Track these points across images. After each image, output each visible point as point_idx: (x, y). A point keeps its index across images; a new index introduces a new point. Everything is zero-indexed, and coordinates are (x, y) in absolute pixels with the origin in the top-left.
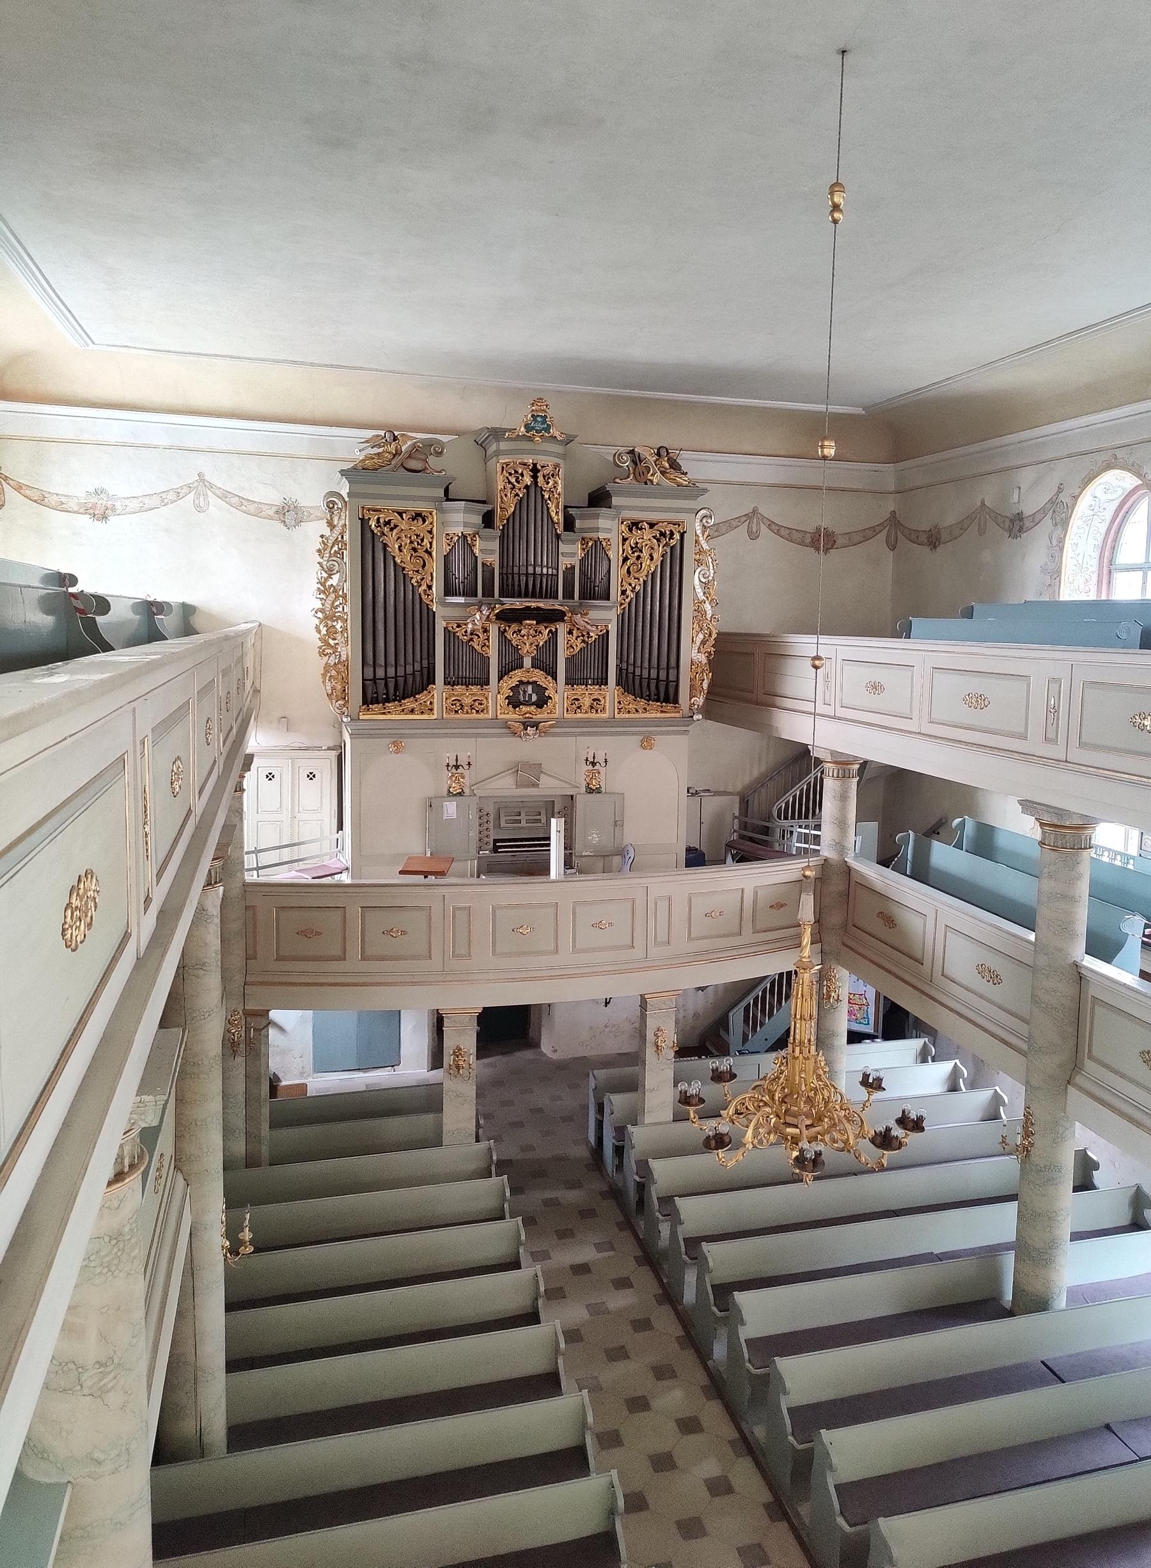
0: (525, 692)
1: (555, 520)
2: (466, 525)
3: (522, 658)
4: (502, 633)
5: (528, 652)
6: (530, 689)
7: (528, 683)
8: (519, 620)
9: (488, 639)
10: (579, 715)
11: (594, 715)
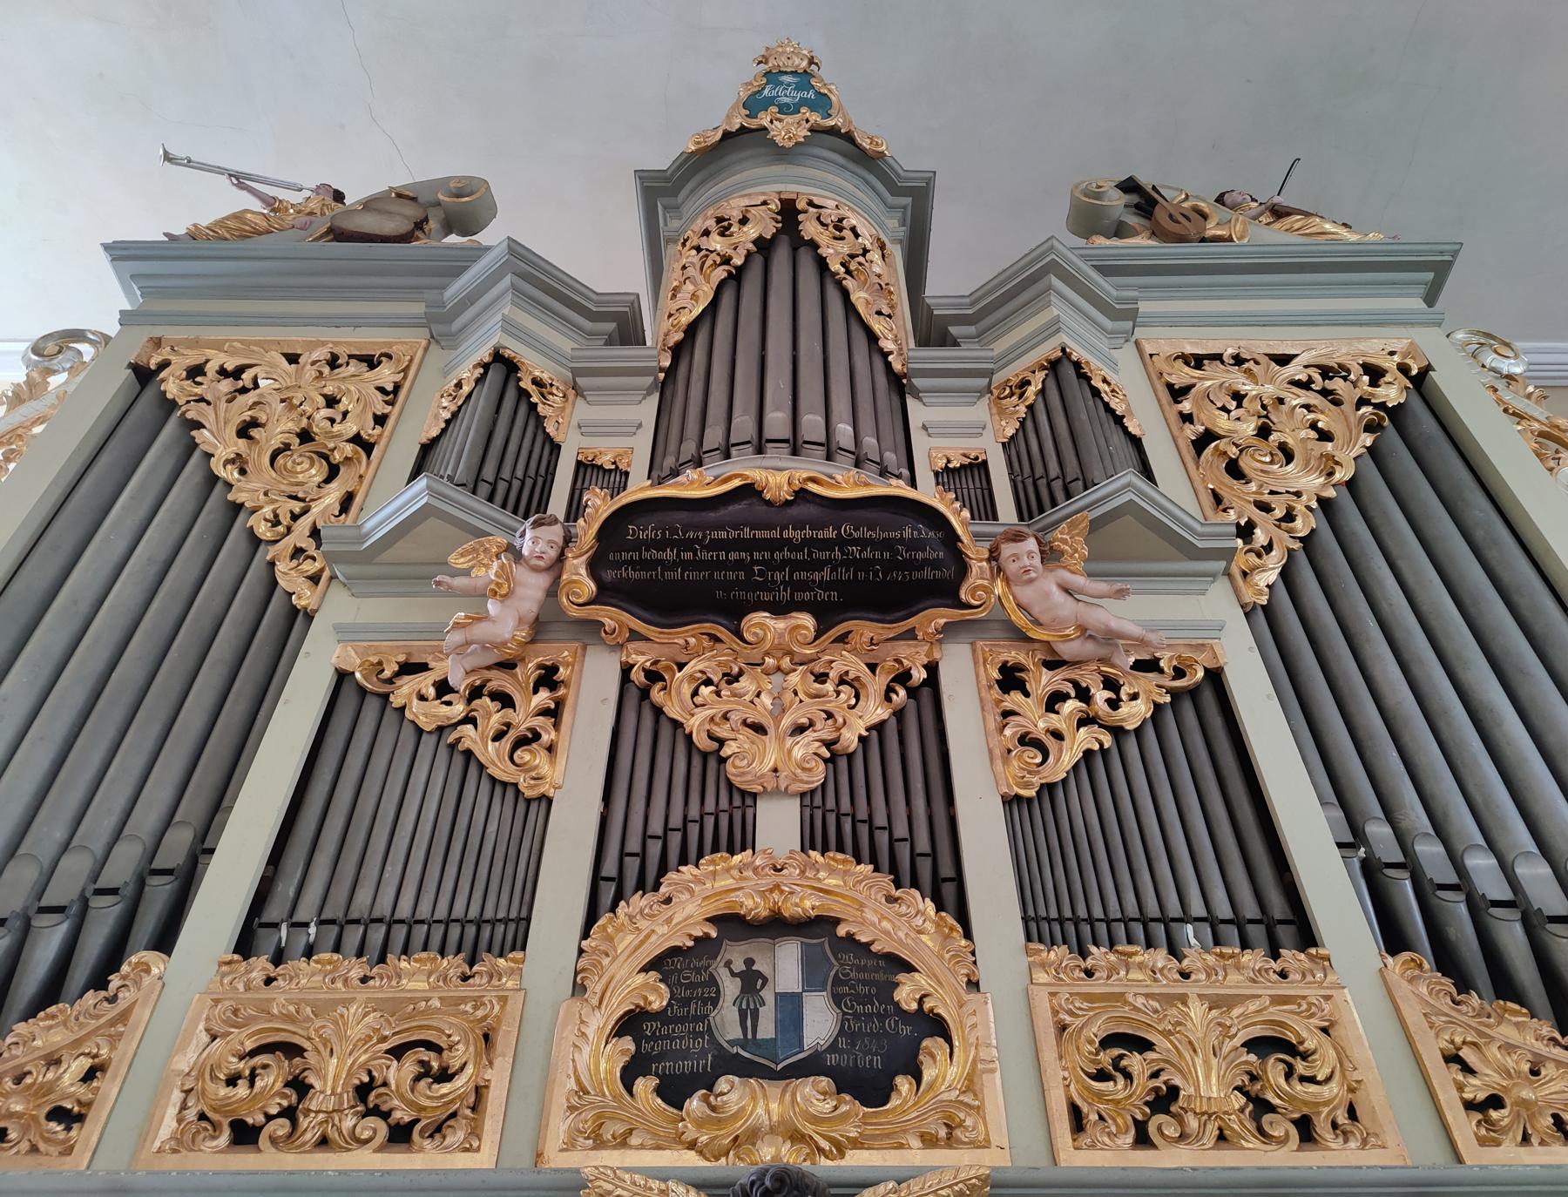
0: (751, 981)
1: (878, 326)
2: (509, 327)
3: (750, 798)
4: (637, 692)
5: (779, 761)
6: (785, 965)
7: (777, 926)
9: (553, 713)
10: (1169, 1159)
11: (1284, 1157)
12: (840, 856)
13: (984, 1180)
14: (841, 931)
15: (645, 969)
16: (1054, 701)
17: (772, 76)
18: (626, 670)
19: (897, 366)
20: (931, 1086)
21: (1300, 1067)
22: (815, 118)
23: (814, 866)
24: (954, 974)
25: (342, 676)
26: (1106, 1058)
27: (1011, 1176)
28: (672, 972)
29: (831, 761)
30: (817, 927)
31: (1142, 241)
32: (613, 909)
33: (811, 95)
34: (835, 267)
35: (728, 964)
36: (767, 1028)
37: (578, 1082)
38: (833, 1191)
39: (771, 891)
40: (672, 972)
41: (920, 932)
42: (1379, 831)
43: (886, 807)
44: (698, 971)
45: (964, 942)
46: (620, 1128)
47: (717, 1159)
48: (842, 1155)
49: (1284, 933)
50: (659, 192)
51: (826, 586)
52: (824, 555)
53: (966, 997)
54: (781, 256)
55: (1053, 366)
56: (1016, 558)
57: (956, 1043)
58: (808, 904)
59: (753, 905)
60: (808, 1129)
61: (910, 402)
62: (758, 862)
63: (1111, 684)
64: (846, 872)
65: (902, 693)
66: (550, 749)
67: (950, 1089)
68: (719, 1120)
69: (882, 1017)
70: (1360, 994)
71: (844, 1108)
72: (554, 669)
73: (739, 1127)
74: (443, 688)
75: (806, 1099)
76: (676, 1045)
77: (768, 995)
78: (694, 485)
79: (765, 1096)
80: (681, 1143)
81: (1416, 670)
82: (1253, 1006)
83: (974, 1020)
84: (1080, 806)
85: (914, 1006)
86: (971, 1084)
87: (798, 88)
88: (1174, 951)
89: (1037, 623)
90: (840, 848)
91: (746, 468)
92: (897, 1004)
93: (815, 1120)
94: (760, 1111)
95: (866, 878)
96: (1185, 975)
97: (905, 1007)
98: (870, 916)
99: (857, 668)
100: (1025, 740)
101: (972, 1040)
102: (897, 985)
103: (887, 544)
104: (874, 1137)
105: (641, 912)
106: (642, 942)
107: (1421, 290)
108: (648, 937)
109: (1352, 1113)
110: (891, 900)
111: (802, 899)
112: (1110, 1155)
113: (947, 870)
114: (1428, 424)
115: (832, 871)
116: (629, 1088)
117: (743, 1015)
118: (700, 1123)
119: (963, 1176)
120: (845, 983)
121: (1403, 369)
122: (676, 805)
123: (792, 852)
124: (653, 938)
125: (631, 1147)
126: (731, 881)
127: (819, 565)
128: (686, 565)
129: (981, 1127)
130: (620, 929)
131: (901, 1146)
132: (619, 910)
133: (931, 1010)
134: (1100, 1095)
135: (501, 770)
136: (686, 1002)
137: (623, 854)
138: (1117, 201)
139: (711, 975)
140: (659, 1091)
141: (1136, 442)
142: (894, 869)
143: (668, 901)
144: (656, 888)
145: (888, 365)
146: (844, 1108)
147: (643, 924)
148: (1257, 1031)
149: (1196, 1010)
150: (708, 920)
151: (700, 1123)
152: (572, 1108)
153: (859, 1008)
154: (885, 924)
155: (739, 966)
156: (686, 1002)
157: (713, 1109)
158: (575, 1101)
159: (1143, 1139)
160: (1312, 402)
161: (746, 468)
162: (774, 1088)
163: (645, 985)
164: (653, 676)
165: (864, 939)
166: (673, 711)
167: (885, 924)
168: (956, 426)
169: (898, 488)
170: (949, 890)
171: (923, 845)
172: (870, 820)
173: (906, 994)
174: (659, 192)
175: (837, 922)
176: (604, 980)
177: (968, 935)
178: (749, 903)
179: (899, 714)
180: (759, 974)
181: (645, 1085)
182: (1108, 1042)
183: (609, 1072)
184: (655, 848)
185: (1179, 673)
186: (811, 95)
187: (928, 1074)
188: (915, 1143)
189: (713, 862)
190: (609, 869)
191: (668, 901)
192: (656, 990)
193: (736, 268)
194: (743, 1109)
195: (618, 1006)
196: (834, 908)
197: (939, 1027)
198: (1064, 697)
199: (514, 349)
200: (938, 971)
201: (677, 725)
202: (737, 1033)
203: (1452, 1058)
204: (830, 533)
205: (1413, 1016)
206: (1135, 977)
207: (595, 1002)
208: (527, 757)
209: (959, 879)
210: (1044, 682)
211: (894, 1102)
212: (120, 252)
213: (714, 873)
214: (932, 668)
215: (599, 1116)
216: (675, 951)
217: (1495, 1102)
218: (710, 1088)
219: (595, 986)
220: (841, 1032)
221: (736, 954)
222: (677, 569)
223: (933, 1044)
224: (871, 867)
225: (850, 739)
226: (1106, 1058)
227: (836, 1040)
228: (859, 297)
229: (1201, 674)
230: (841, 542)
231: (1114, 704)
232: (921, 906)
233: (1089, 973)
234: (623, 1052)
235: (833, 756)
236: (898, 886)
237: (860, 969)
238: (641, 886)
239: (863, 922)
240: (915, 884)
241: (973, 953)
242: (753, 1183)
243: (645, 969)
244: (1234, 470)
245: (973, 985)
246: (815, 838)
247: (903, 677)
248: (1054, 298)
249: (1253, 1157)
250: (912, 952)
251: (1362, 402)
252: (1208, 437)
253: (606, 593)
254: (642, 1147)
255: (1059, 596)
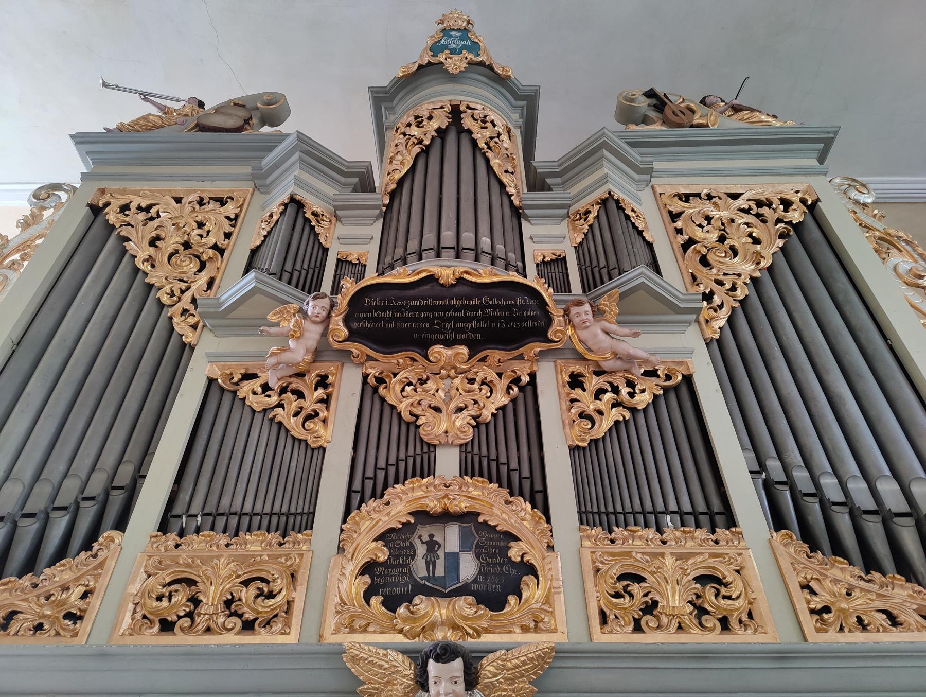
0: (432, 546)
1: (505, 179)
2: (298, 182)
3: (432, 447)
4: (371, 389)
5: (448, 428)
6: (450, 537)
7: (446, 517)
8: (420, 343)
9: (326, 401)
10: (651, 638)
11: (713, 638)
12: (480, 479)
13: (552, 649)
14: (481, 519)
15: (376, 540)
16: (599, 394)
17: (446, 32)
18: (365, 377)
19: (516, 203)
20: (527, 601)
21: (723, 591)
22: (471, 56)
23: (467, 484)
24: (541, 542)
25: (211, 381)
26: (620, 586)
27: (566, 647)
28: (390, 541)
29: (476, 427)
30: (467, 517)
31: (657, 127)
32: (359, 508)
33: (469, 43)
34: (482, 144)
35: (420, 537)
36: (440, 571)
37: (341, 598)
38: (473, 655)
39: (443, 498)
40: (390, 541)
41: (523, 520)
42: (773, 464)
43: (506, 453)
44: (404, 541)
45: (546, 525)
46: (363, 623)
47: (414, 638)
48: (479, 636)
49: (719, 519)
50: (383, 99)
51: (473, 331)
52: (473, 314)
53: (546, 554)
54: (451, 138)
55: (604, 202)
56: (578, 315)
57: (541, 578)
58: (463, 505)
59: (433, 505)
60: (461, 623)
61: (524, 223)
62: (436, 483)
63: (630, 384)
64: (484, 488)
65: (516, 389)
66: (324, 421)
67: (537, 602)
68: (415, 618)
69: (501, 565)
70: (758, 550)
71: (481, 612)
72: (325, 377)
73: (425, 622)
74: (266, 388)
75: (460, 608)
76: (393, 579)
77: (441, 553)
78: (400, 275)
79: (439, 606)
80: (395, 630)
81: (800, 375)
82: (699, 559)
83: (550, 566)
84: (612, 451)
85: (519, 559)
86: (548, 600)
87: (461, 39)
88: (659, 530)
89: (590, 350)
90: (481, 475)
91: (430, 266)
92: (510, 558)
93: (465, 618)
94: (436, 613)
95: (495, 491)
96: (664, 542)
97: (514, 559)
98: (496, 511)
99: (491, 375)
100: (582, 415)
101: (549, 576)
102: (510, 548)
103: (508, 308)
104: (496, 627)
105: (374, 509)
106: (374, 525)
107: (816, 154)
108: (377, 522)
109: (750, 615)
110: (507, 502)
111: (460, 502)
112: (621, 636)
113: (538, 487)
114: (816, 234)
115: (476, 487)
116: (368, 602)
117: (427, 563)
118: (405, 620)
119: (540, 647)
120: (482, 547)
121: (803, 201)
122: (392, 451)
123: (455, 477)
124: (380, 523)
125: (369, 632)
126: (368, 523)
127: (470, 320)
128: (397, 320)
129: (553, 622)
130: (362, 518)
131: (510, 632)
132: (362, 508)
133: (528, 561)
134: (616, 606)
135: (298, 433)
136: (397, 557)
137: (364, 478)
138: (643, 103)
139: (411, 543)
140: (384, 603)
141: (650, 245)
142: (510, 486)
143: (388, 503)
144: (382, 496)
145: (511, 202)
146: (481, 612)
147: (375, 516)
148: (702, 572)
149: (669, 561)
150: (409, 513)
151: (405, 620)
152: (338, 612)
153: (489, 560)
154: (504, 516)
155: (426, 538)
156: (397, 557)
157: (412, 613)
158: (339, 608)
159: (638, 628)
160: (750, 221)
161: (430, 266)
162: (444, 602)
163: (376, 548)
164: (380, 380)
165: (492, 524)
166: (391, 400)
167: (504, 516)
168: (549, 237)
169: (513, 276)
170: (539, 497)
171: (526, 473)
172: (497, 459)
173: (514, 553)
174: (383, 99)
175: (479, 514)
176: (354, 545)
177: (549, 521)
178: (431, 505)
179: (514, 401)
180: (436, 542)
181: (376, 601)
182: (621, 578)
183: (357, 593)
184: (381, 475)
185: (668, 377)
186: (469, 43)
187: (525, 595)
188: (518, 630)
189: (412, 483)
190: (357, 486)
191: (388, 503)
192: (382, 551)
193: (426, 146)
194: (427, 612)
195: (362, 559)
196: (477, 508)
197: (531, 570)
198: (604, 391)
199: (302, 195)
200: (532, 541)
201: (393, 407)
202: (425, 573)
203: (806, 587)
204: (476, 302)
205: (785, 564)
206: (637, 543)
207: (349, 557)
208: (312, 426)
209: (545, 491)
210: (593, 383)
211: (507, 609)
212: (80, 139)
213: (413, 488)
214: (533, 375)
215: (352, 616)
216: (392, 530)
217: (827, 609)
218: (410, 602)
219: (349, 549)
220: (480, 573)
221: (424, 532)
222: (392, 322)
223: (528, 579)
224: (497, 485)
225: (487, 415)
226: (620, 586)
227: (477, 577)
228: (495, 162)
229: (680, 378)
230: (483, 307)
231: (632, 395)
232: (524, 506)
233: (613, 541)
234: (364, 583)
235: (478, 424)
236: (512, 495)
237: (490, 539)
238: (374, 495)
239: (492, 515)
240: (521, 494)
241: (551, 531)
242: (431, 651)
243: (376, 540)
244: (704, 261)
245: (551, 548)
246: (466, 469)
247: (516, 381)
248: (605, 162)
249: (696, 638)
250: (518, 530)
251: (779, 221)
252: (691, 242)
253: (353, 335)
254: (375, 632)
255: (602, 336)
